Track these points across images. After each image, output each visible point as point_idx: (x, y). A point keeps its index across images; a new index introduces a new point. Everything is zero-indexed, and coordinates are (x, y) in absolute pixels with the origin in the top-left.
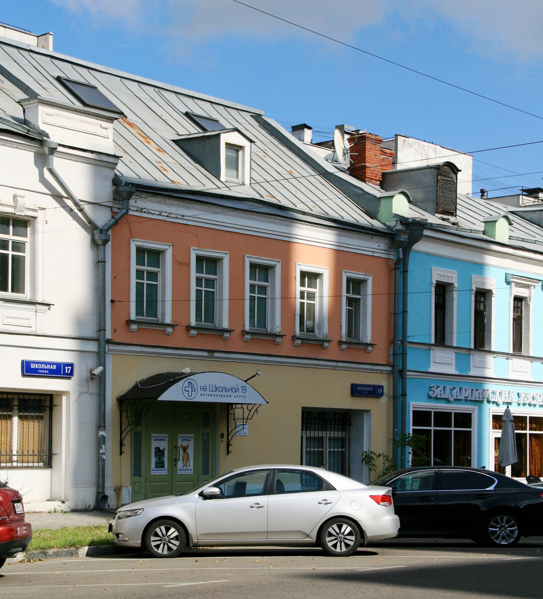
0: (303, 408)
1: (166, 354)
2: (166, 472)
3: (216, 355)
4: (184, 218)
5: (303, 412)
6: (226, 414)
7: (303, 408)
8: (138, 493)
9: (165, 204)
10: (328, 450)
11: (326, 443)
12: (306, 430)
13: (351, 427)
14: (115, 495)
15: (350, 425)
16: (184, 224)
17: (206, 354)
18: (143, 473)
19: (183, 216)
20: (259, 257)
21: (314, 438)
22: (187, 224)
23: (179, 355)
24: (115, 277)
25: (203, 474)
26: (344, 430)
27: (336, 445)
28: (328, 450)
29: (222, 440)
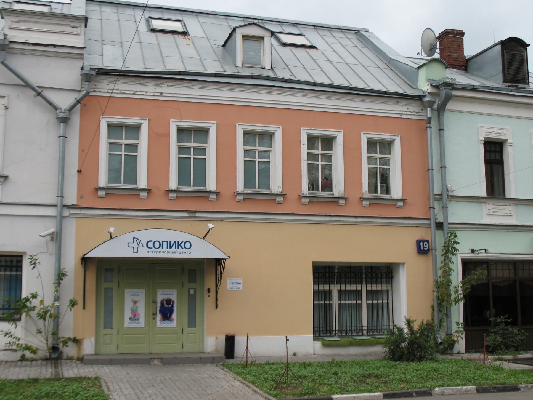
0: (313, 263)
1: (137, 216)
3: (198, 215)
4: (163, 95)
5: (314, 267)
6: (214, 270)
7: (314, 263)
8: (110, 344)
9: (141, 84)
12: (366, 284)
13: (393, 280)
15: (392, 278)
17: (186, 215)
18: (115, 325)
19: (162, 93)
21: (346, 291)
23: (153, 216)
25: (189, 326)
26: (388, 283)
27: (320, 299)
28: (338, 302)
29: (210, 294)
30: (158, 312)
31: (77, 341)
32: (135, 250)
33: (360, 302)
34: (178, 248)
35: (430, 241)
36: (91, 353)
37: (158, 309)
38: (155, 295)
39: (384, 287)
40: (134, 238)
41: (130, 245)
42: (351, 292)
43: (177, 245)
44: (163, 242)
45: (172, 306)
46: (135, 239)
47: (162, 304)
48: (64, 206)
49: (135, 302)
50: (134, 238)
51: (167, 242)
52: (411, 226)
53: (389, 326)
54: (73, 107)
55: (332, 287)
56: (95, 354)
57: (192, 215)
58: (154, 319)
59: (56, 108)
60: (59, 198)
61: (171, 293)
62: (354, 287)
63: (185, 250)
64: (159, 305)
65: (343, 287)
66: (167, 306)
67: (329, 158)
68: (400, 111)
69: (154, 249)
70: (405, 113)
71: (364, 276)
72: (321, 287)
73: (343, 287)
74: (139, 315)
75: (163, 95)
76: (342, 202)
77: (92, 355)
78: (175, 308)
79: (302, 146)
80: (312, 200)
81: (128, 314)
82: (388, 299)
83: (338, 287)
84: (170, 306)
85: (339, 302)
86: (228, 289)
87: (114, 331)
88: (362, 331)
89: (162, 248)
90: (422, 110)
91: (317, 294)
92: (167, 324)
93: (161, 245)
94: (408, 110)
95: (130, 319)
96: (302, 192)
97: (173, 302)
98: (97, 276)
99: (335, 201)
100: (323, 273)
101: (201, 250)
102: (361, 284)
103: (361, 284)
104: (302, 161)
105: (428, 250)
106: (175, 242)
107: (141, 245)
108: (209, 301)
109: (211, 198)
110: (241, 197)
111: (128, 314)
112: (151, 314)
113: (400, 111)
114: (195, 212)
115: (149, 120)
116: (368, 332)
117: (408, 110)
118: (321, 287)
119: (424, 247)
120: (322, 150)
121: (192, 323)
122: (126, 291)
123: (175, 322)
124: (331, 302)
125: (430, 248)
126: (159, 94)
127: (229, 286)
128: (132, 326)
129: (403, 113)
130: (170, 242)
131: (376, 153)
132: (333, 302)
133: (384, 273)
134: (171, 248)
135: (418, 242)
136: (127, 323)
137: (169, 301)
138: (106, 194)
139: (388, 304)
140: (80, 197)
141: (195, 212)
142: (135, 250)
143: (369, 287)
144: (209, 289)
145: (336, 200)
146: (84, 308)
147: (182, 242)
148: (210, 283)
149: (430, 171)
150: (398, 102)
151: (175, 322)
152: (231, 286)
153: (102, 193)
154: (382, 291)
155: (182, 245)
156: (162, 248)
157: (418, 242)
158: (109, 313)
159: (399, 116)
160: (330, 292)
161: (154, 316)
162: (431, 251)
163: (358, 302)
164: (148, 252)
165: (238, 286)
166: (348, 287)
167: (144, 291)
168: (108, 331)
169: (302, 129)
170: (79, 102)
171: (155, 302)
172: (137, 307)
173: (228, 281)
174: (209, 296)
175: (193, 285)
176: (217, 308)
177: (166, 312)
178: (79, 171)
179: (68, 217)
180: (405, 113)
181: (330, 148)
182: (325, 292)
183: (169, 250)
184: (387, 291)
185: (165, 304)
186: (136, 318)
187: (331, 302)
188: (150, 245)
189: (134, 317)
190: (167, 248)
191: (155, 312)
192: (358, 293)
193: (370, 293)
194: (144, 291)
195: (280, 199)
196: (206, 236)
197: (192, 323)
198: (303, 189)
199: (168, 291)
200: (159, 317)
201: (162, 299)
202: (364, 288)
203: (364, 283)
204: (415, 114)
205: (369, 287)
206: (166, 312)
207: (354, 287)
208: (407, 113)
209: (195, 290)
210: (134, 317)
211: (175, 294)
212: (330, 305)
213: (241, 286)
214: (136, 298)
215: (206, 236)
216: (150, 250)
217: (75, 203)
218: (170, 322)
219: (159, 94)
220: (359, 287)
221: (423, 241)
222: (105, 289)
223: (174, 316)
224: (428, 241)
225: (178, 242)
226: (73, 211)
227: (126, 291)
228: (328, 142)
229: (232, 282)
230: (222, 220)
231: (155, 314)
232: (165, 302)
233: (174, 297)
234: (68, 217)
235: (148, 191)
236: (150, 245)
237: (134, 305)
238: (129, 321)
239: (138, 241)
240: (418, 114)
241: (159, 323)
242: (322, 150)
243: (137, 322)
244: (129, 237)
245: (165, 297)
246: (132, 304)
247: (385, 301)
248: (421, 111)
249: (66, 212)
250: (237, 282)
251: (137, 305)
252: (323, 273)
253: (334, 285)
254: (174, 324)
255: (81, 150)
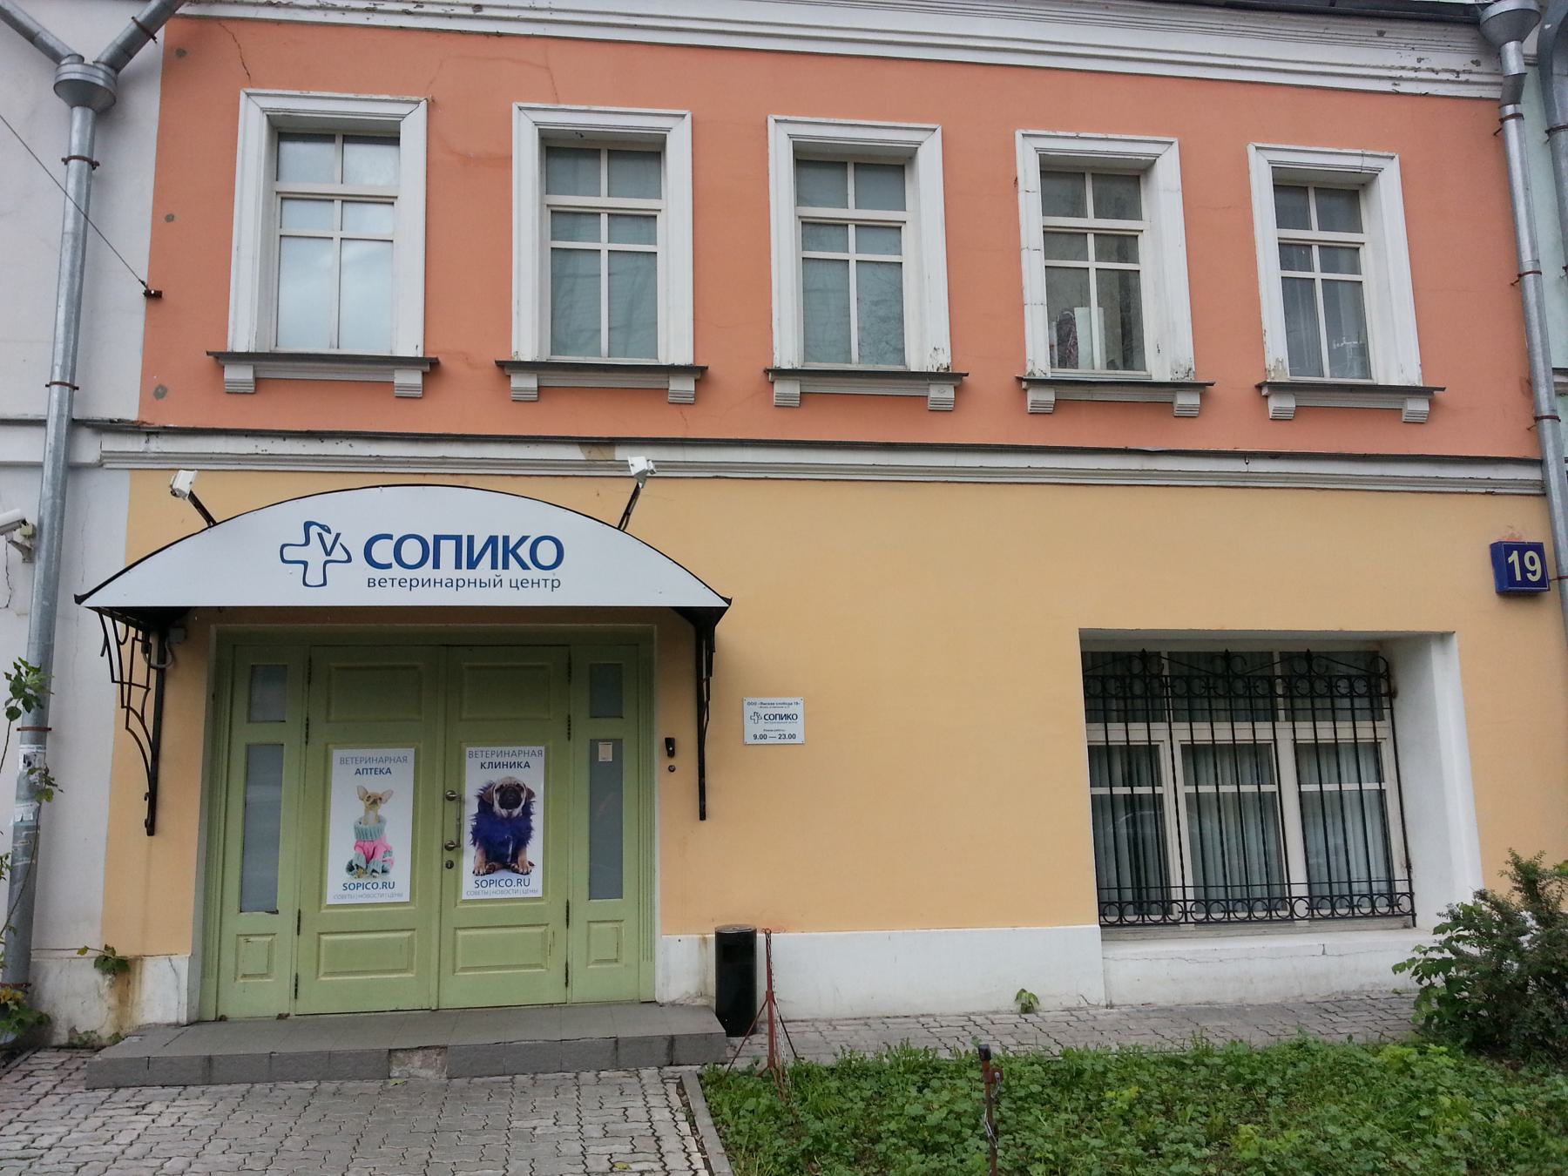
1: (379, 460)
2: (402, 891)
10: (1184, 790)
11: (1170, 765)
13: (1397, 703)
14: (105, 990)
15: (1392, 694)
16: (487, 34)
17: (575, 453)
18: (286, 898)
19: (478, 7)
20: (832, 121)
22: (499, 35)
23: (443, 461)
24: (170, 218)
26: (1376, 715)
29: (672, 762)
30: (467, 838)
31: (118, 967)
32: (314, 576)
33: (1274, 788)
34: (506, 566)
35: (1548, 550)
36: (173, 1019)
37: (468, 825)
38: (457, 771)
39: (1365, 732)
40: (308, 525)
41: (290, 554)
42: (1234, 749)
43: (502, 550)
44: (437, 539)
45: (527, 812)
46: (314, 530)
47: (485, 803)
48: (76, 424)
49: (374, 801)
50: (308, 525)
51: (458, 539)
52: (1464, 490)
53: (1390, 881)
54: (127, 50)
55: (1160, 731)
56: (189, 1024)
57: (597, 454)
58: (450, 865)
59: (55, 57)
60: (56, 388)
61: (522, 759)
62: (1244, 733)
63: (535, 573)
64: (472, 808)
65: (1202, 733)
66: (504, 812)
67: (1124, 246)
68: (1391, 68)
69: (397, 571)
70: (1412, 74)
71: (1280, 691)
72: (1117, 733)
73: (1202, 733)
74: (388, 851)
75: (486, 12)
76: (1186, 400)
77: (178, 1025)
78: (537, 821)
79: (1021, 196)
80: (1070, 394)
81: (342, 849)
82: (1380, 780)
83: (1182, 732)
84: (517, 811)
85: (1192, 789)
86: (749, 740)
87: (285, 921)
88: (1287, 901)
89: (436, 565)
90: (1477, 63)
91: (1099, 756)
92: (503, 887)
93: (431, 552)
94: (1423, 65)
95: (350, 868)
96: (1029, 368)
97: (531, 794)
98: (215, 698)
99: (1158, 397)
100: (1127, 677)
101: (606, 570)
102: (1274, 719)
103: (1274, 719)
104: (1024, 253)
105: (1543, 582)
106: (492, 540)
107: (338, 554)
108: (671, 790)
109: (676, 393)
110: (791, 388)
111: (342, 849)
112: (437, 846)
113: (1391, 68)
114: (612, 442)
115: (431, 105)
116: (1310, 908)
117: (1423, 65)
118: (1117, 733)
119: (1524, 570)
120: (1097, 215)
121: (606, 877)
122: (337, 754)
123: (536, 875)
124: (1158, 790)
125: (1551, 574)
126: (469, 11)
127: (752, 729)
128: (358, 896)
129: (1404, 74)
130: (471, 539)
131: (1307, 227)
132: (1165, 790)
133: (1358, 678)
134: (472, 564)
135: (1500, 552)
136: (337, 885)
137: (513, 794)
138: (257, 380)
139: (1381, 793)
140: (157, 393)
141: (612, 442)
142: (314, 576)
143: (1305, 732)
144: (670, 742)
145: (1161, 396)
146: (151, 827)
147: (524, 539)
148: (675, 719)
149: (1530, 277)
150: (1381, 34)
151: (536, 875)
152: (761, 727)
153: (240, 375)
154: (1335, 748)
155: (524, 551)
156: (436, 565)
157: (1500, 552)
158: (260, 843)
159: (1387, 86)
160: (1152, 751)
161: (449, 856)
162: (1554, 585)
163: (1266, 788)
164: (371, 583)
165: (787, 727)
166: (1223, 733)
167: (410, 753)
168: (256, 920)
169: (1018, 134)
170: (144, 31)
171: (455, 798)
172: (380, 820)
173: (749, 711)
174: (671, 769)
175: (609, 728)
176: (703, 816)
177: (501, 840)
178: (153, 296)
179: (100, 465)
180: (1412, 74)
181: (1131, 208)
182: (1129, 750)
183: (464, 573)
184: (1375, 747)
185: (496, 806)
186: (376, 864)
187: (1158, 790)
188: (383, 552)
189: (368, 863)
190: (458, 566)
191: (451, 836)
192: (1260, 757)
193: (1310, 754)
194: (410, 753)
195: (941, 393)
196: (627, 513)
197: (606, 877)
198: (1029, 356)
199: (507, 753)
200: (471, 857)
201: (482, 783)
202: (1284, 736)
203: (1282, 714)
204: (1452, 77)
205: (1305, 732)
206: (501, 840)
207: (1244, 733)
208: (1420, 75)
209: (617, 745)
210: (368, 863)
211: (538, 764)
212: (1157, 801)
213: (797, 728)
214: (375, 785)
215: (627, 513)
216: (378, 574)
217: (132, 415)
218: (515, 877)
219: (469, 11)
220: (1264, 732)
221: (1522, 548)
222: (249, 748)
223: (534, 851)
224: (1538, 548)
225: (506, 539)
226: (113, 444)
227: (337, 754)
228: (1123, 182)
229: (762, 712)
230: (719, 473)
231: (454, 847)
232: (496, 797)
233: (533, 778)
234: (100, 465)
235: (430, 367)
236: (383, 552)
237: (368, 810)
238: (347, 878)
239: (329, 539)
240: (1463, 77)
241: (471, 882)
242: (1097, 215)
243: (380, 879)
244: (287, 522)
245: (499, 777)
246: (360, 808)
247: (1350, 786)
248: (1475, 68)
249: (90, 448)
250: (783, 712)
251: (383, 810)
252: (1127, 677)
253: (1165, 725)
254: (535, 883)
255: (164, 218)
